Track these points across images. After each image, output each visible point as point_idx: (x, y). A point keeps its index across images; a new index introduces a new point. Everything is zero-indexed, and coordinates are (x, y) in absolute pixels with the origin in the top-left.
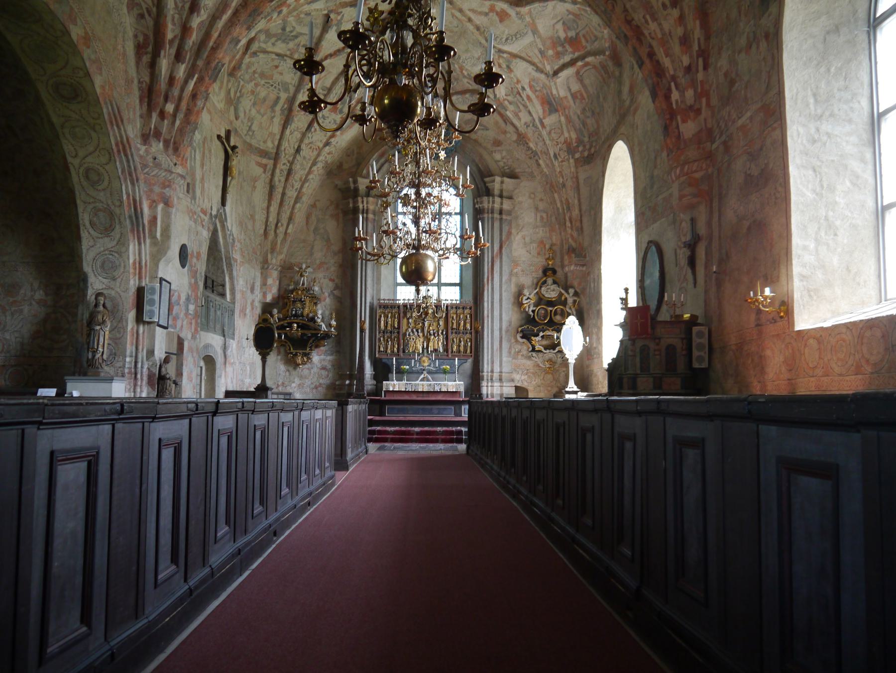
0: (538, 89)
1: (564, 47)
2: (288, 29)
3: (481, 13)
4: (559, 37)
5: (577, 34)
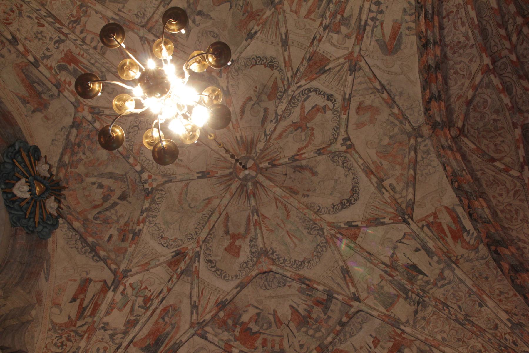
0: (167, 319)
1: (235, 325)
2: (198, 18)
3: (226, 226)
4: (240, 316)
5: (259, 332)
